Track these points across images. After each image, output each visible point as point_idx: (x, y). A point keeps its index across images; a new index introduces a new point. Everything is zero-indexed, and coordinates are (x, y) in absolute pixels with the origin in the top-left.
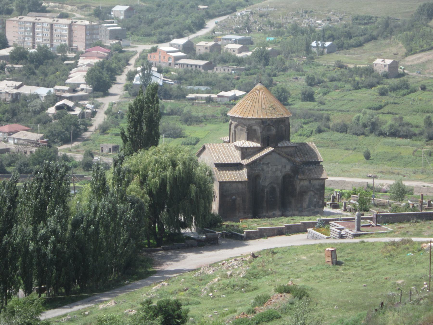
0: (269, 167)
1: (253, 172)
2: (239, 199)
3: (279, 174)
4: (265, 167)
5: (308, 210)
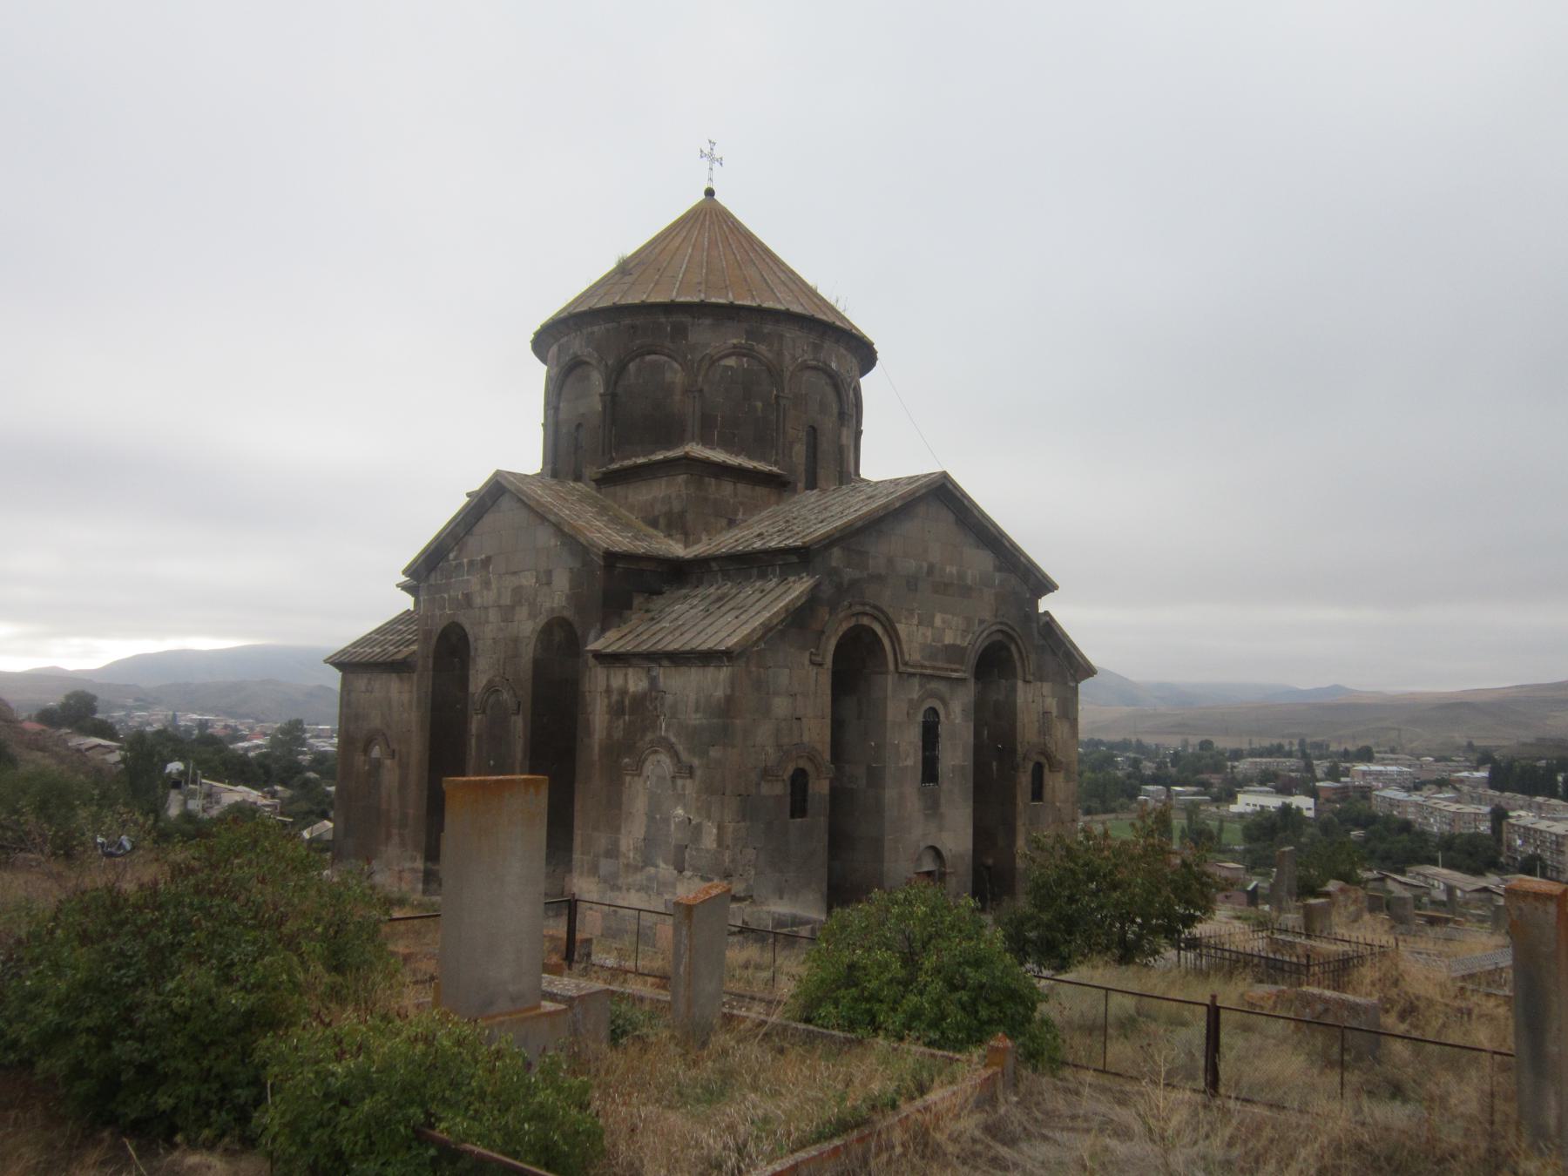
0: (486, 584)
1: (438, 612)
2: (388, 762)
3: (527, 627)
4: (474, 582)
5: (639, 877)
